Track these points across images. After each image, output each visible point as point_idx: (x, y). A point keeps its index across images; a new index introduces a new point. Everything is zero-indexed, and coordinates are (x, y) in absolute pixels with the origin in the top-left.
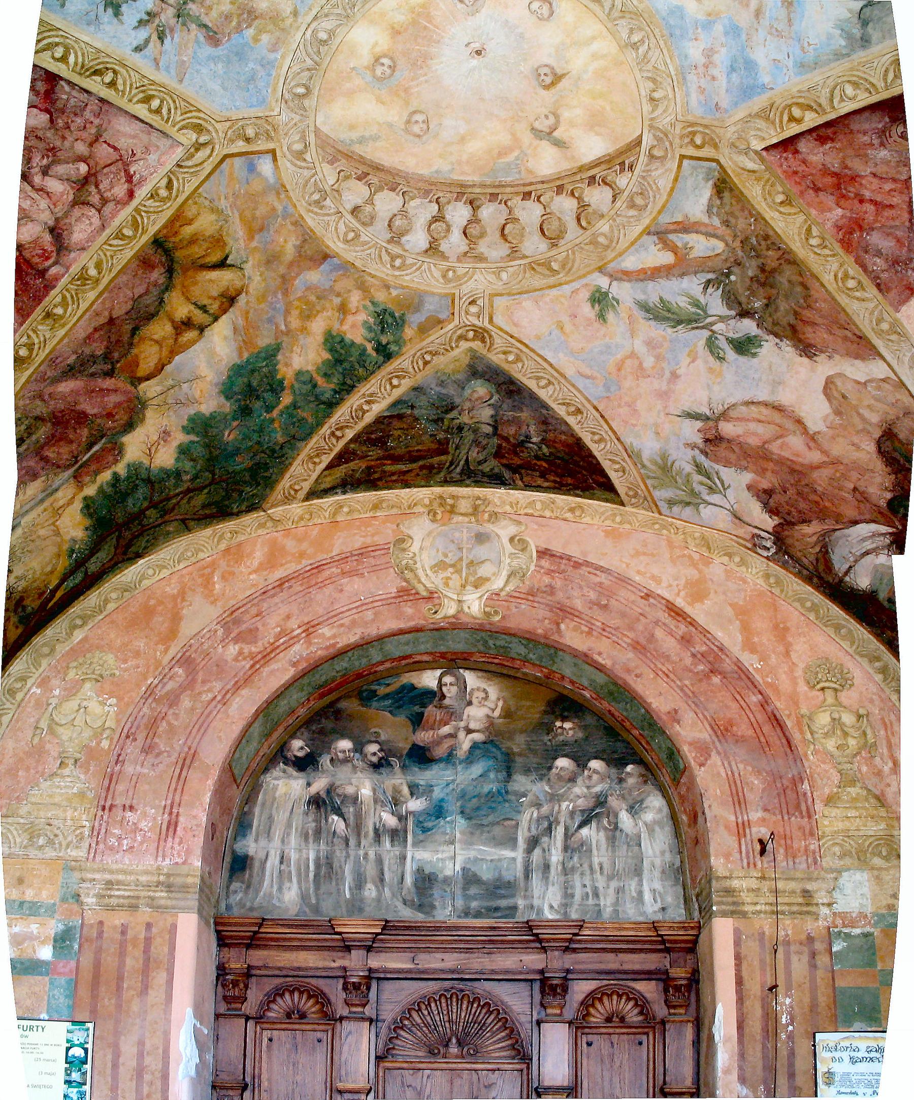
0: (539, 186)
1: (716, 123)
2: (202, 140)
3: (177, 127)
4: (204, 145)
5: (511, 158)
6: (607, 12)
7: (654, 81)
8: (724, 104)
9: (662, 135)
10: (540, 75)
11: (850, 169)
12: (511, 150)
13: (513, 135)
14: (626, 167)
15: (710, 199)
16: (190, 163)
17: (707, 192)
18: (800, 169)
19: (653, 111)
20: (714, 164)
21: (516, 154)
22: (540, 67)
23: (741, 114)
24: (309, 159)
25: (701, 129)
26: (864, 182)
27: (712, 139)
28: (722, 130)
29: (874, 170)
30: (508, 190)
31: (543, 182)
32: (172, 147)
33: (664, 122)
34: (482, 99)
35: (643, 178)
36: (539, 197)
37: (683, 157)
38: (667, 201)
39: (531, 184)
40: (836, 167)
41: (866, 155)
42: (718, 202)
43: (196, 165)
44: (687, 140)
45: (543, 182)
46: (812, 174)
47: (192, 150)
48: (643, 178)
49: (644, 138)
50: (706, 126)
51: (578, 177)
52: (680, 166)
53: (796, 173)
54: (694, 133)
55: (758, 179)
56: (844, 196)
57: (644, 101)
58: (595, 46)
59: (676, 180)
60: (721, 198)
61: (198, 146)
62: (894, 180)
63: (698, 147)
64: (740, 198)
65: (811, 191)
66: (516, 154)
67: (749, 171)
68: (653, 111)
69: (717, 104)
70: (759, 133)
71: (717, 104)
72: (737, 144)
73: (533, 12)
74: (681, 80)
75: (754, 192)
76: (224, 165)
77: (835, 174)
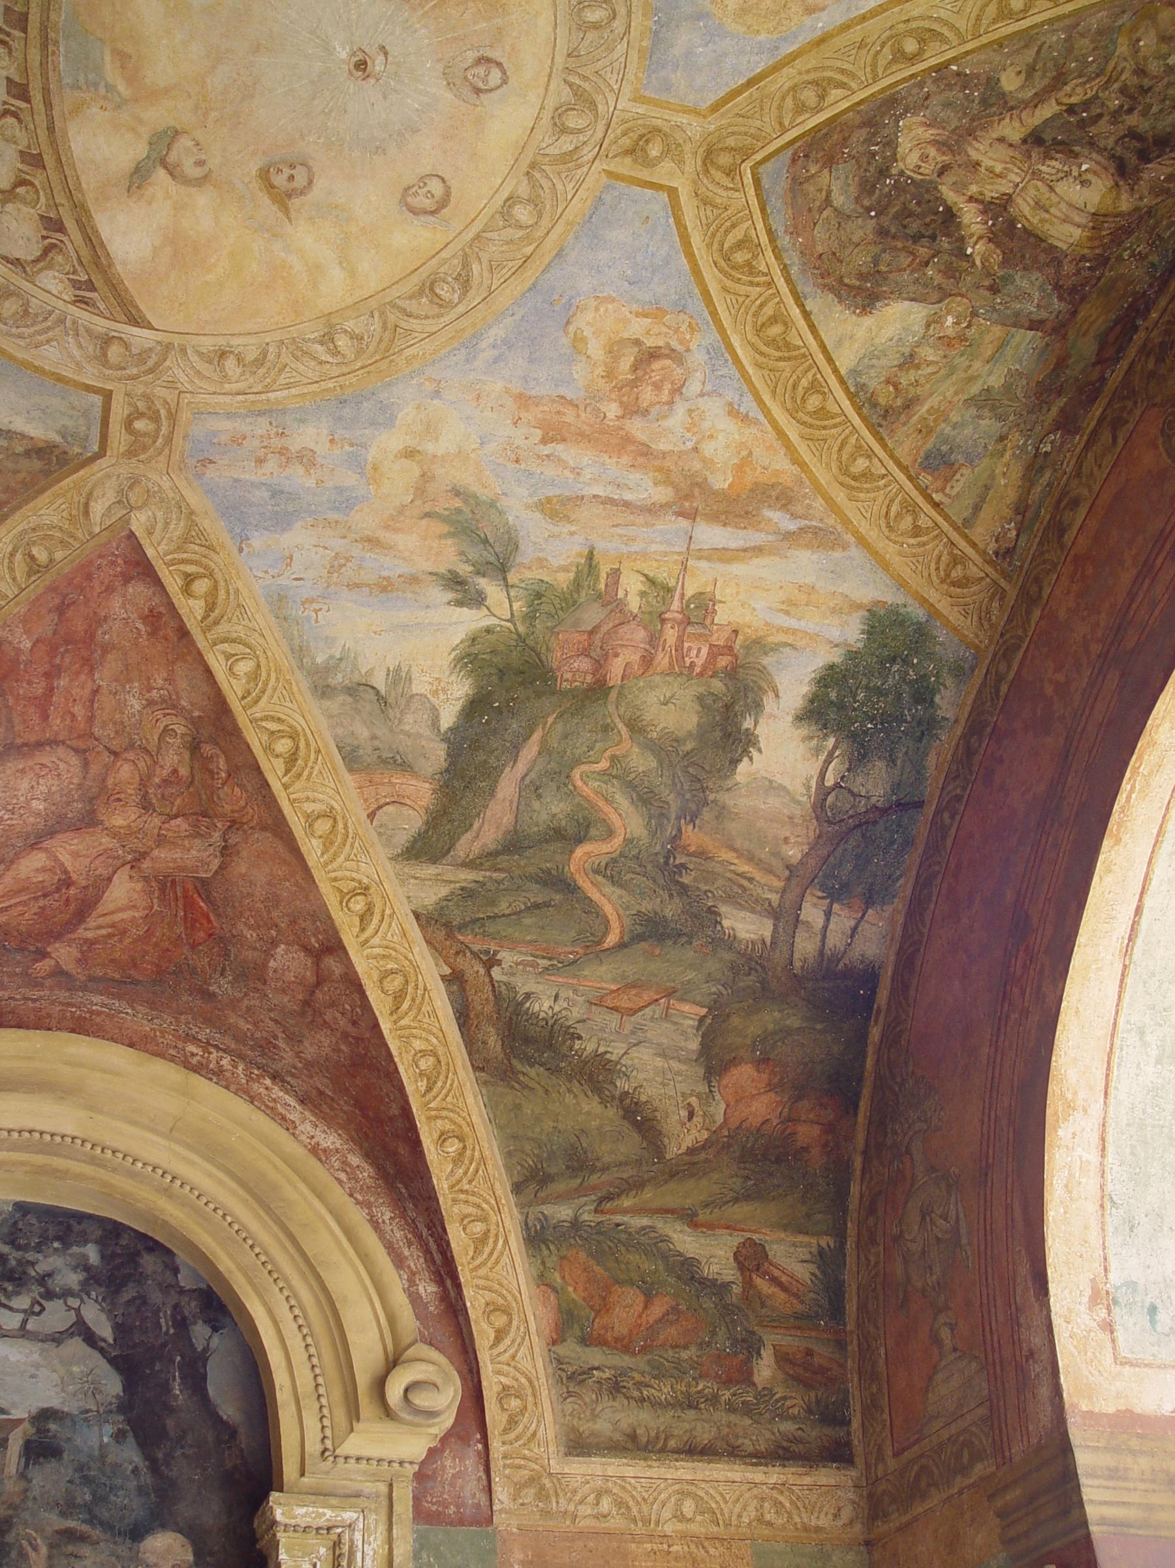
0: (41, 119)
1: (176, 457)
5: (111, 72)
6: (399, 302)
7: (260, 361)
8: (210, 472)
9: (150, 363)
10: (292, 166)
11: (103, 656)
12: (133, 79)
13: (166, 91)
14: (83, 292)
15: (23, 436)
17: (37, 431)
18: (96, 583)
19: (200, 354)
20: (96, 448)
21: (121, 87)
22: (309, 169)
23: (194, 499)
25: (164, 430)
26: (83, 677)
27: (145, 448)
28: (162, 466)
29: (105, 691)
30: (35, 56)
31: (51, 129)
33: (176, 369)
34: (257, 49)
35: (62, 321)
36: (15, 115)
37: (108, 396)
38: (12, 358)
39: (48, 105)
40: (103, 636)
41: (130, 681)
42: (20, 449)
44: (141, 405)
45: (51, 129)
46: (87, 601)
48: (62, 321)
49: (145, 333)
50: (169, 440)
51: (60, 199)
52: (88, 388)
53: (89, 577)
54: (156, 419)
55: (71, 519)
56: (53, 650)
57: (222, 341)
58: (337, 274)
59: (59, 378)
60: (27, 453)
62: (91, 719)
63: (128, 424)
64: (31, 488)
65: (57, 601)
66: (121, 87)
67: (87, 505)
68: (200, 354)
69: (211, 462)
70: (160, 526)
71: (211, 462)
72: (137, 489)
73: (423, 180)
74: (259, 407)
75: (47, 510)
77: (90, 637)
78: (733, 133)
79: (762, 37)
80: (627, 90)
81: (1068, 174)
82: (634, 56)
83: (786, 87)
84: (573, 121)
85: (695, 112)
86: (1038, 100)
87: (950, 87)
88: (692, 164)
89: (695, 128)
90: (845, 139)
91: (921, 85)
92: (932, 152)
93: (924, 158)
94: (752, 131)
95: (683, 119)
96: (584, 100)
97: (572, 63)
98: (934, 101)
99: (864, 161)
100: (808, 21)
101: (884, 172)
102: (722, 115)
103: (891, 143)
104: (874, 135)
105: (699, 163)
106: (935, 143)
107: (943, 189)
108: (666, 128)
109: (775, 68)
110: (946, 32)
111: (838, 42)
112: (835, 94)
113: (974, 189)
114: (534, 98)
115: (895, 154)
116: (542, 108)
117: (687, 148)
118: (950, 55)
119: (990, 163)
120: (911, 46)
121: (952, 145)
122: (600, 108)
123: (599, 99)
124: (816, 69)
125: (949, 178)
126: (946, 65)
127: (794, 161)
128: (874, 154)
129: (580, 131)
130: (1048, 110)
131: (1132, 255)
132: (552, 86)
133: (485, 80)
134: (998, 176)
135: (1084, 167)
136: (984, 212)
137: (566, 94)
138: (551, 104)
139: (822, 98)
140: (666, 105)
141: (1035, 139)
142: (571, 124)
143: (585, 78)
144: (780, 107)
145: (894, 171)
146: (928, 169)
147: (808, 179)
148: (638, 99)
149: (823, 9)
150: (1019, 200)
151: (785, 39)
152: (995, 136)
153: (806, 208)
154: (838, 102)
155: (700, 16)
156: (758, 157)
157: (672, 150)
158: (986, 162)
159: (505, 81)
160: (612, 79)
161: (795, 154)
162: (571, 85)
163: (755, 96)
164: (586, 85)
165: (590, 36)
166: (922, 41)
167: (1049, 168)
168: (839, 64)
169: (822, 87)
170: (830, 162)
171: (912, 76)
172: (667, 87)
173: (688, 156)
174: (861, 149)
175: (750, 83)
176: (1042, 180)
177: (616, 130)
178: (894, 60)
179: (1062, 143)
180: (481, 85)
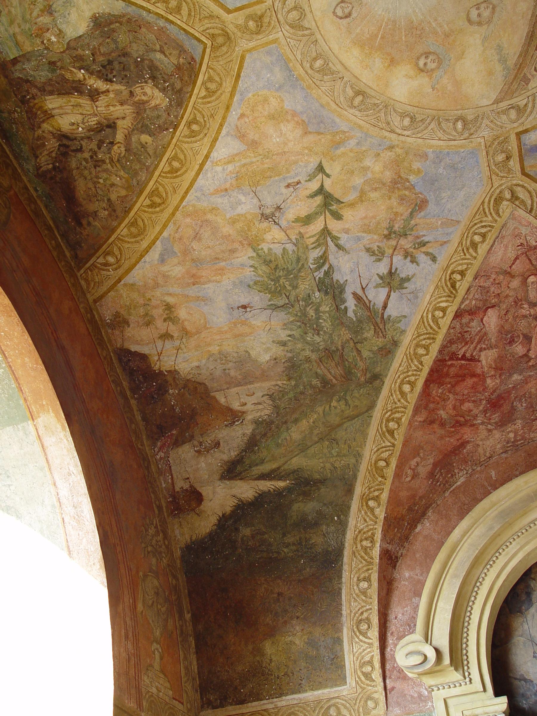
2: (508, 196)
3: (497, 218)
4: (513, 193)
16: (529, 202)
24: (525, 102)
32: (514, 219)
43: (531, 196)
47: (517, 203)
61: (514, 197)
76: (532, 173)
78: (227, 53)
79: (250, 95)
80: (283, 41)
81: (83, 123)
82: (291, 57)
83: (224, 83)
84: (294, 15)
85: (249, 51)
86: (128, 137)
87: (165, 123)
88: (231, 29)
89: (244, 44)
90: (182, 80)
91: (176, 117)
92: (144, 98)
93: (145, 94)
94: (220, 59)
95: (251, 44)
96: (296, 26)
97: (313, 38)
98: (165, 115)
99: (166, 77)
100: (240, 111)
101: (153, 78)
102: (238, 57)
103: (163, 90)
104: (173, 89)
105: (229, 31)
106: (147, 102)
107: (123, 88)
108: (254, 36)
109: (235, 87)
110: (189, 140)
111: (222, 112)
112: (203, 93)
113: (112, 95)
114: (318, 14)
115: (157, 88)
116: (311, 11)
117: (239, 34)
118: (178, 133)
119: (117, 108)
120: (195, 127)
121: (140, 108)
122: (288, 27)
123: (291, 31)
124: (219, 97)
125: (126, 93)
126: (176, 128)
127: (193, 59)
128: (165, 82)
129: (289, 12)
130: (120, 137)
131: (15, 111)
132: (314, 23)
133: (342, 8)
134: (108, 106)
135: (80, 129)
136: (96, 90)
137: (306, 24)
138: (309, 16)
139: (207, 89)
140: (263, 46)
141: (112, 126)
142: (295, 13)
143: (303, 36)
144: (219, 75)
145: (150, 81)
146: (138, 90)
147: (180, 55)
148: (275, 41)
149: (238, 119)
150: (88, 102)
151: (241, 100)
152: (128, 118)
153: (167, 43)
154: (199, 91)
155: (280, 87)
156: (208, 50)
157: (244, 29)
158: (119, 107)
159: (334, 13)
160: (292, 42)
161: (195, 61)
162: (307, 29)
163: (232, 72)
164: (301, 33)
165: (314, 54)
166: (193, 131)
167: (93, 121)
168: (213, 104)
169: (210, 93)
170: (179, 68)
171: (182, 118)
172: (269, 53)
173: (236, 31)
174: (172, 81)
175: (238, 76)
176: (90, 115)
177: (274, 22)
178: (195, 118)
179: (100, 131)
180: (343, 5)
